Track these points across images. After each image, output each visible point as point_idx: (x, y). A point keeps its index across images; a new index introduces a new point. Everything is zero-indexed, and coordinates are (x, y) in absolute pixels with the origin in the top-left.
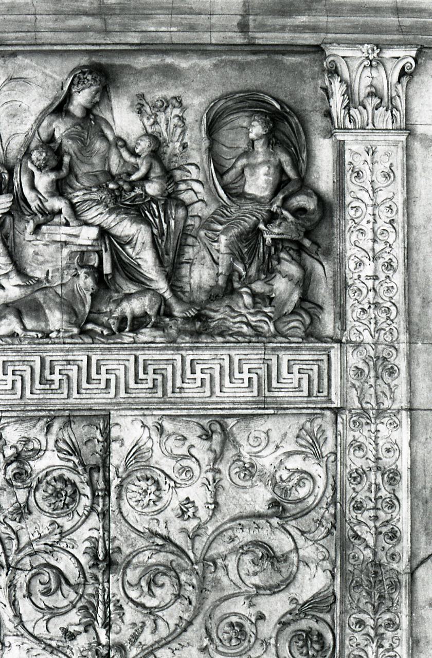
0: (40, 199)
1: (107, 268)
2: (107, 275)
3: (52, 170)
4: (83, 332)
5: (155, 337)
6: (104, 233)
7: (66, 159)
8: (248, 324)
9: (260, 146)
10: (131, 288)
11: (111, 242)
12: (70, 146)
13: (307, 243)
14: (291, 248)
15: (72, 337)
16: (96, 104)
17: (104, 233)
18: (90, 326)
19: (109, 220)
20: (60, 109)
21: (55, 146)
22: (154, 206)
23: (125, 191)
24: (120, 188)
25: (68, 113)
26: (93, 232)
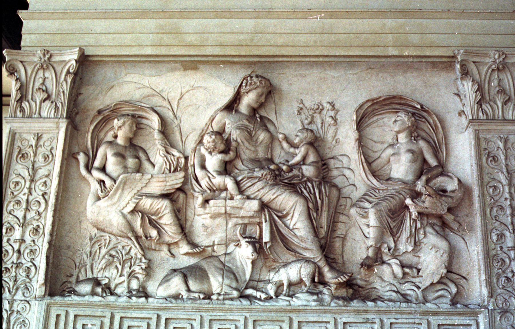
0: (209, 178)
1: (266, 238)
2: (266, 243)
3: (221, 152)
4: (242, 296)
5: (308, 301)
6: (264, 206)
7: (234, 144)
8: (397, 292)
9: (403, 138)
10: (288, 257)
11: (272, 219)
12: (236, 135)
13: (449, 218)
14: (434, 224)
15: (232, 299)
16: (262, 105)
17: (264, 206)
18: (249, 291)
19: (269, 195)
20: (231, 107)
21: (225, 136)
22: (310, 185)
23: (284, 172)
24: (280, 169)
25: (237, 111)
26: (254, 205)
